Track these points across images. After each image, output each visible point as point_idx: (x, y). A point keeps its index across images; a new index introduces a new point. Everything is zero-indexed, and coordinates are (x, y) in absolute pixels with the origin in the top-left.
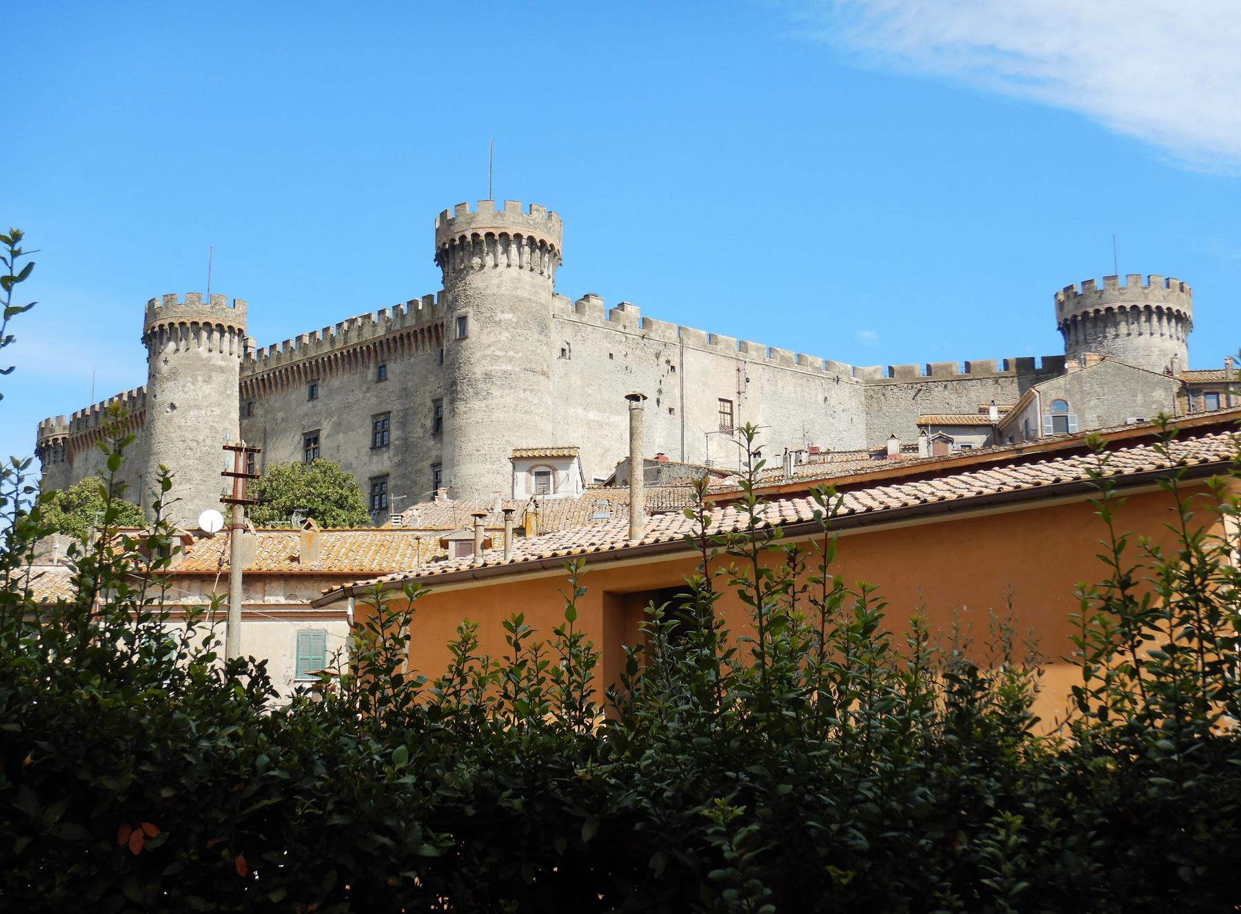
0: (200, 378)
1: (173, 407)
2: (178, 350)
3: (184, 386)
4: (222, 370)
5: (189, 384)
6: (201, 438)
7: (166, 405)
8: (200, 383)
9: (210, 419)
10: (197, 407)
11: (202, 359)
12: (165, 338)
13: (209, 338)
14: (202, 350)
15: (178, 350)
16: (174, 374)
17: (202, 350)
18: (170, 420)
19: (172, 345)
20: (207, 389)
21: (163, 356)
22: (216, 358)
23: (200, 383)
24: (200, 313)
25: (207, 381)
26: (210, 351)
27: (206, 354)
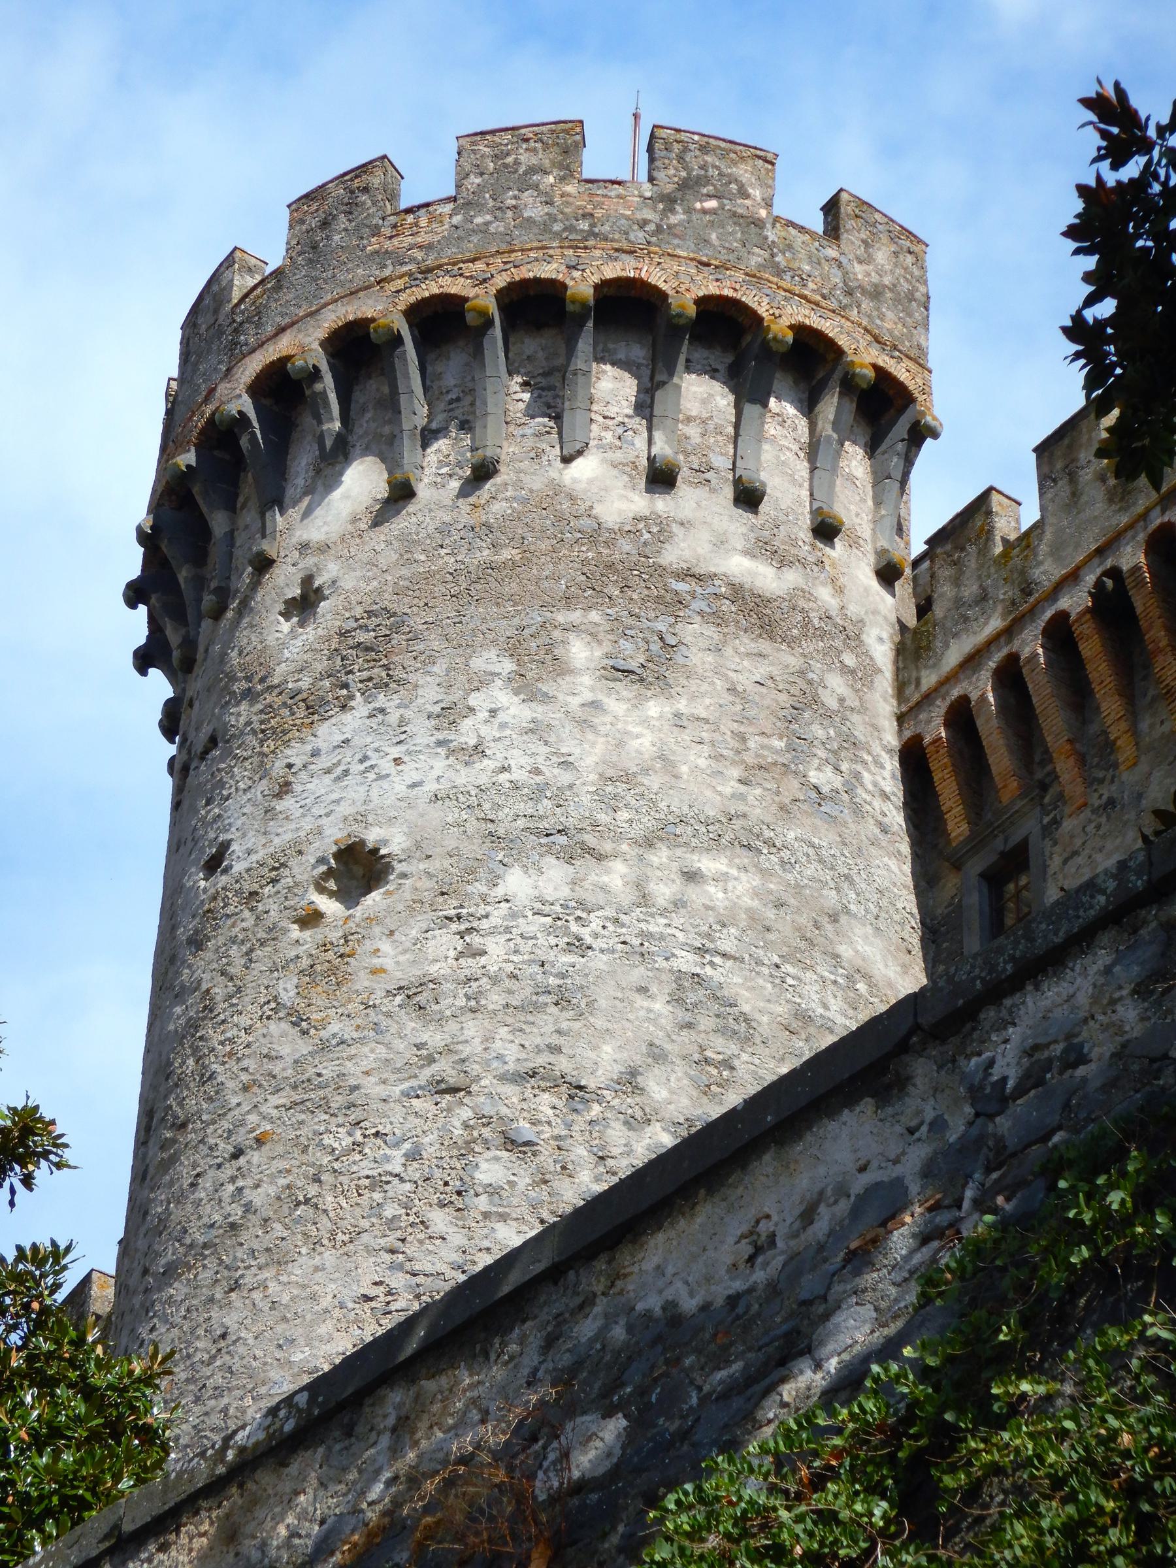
0: (579, 652)
1: (359, 868)
2: (401, 493)
3: (449, 714)
4: (756, 614)
5: (502, 696)
6: (602, 1062)
7: (303, 869)
8: (585, 686)
9: (679, 931)
10: (577, 847)
11: (596, 534)
12: (302, 461)
13: (645, 407)
14: (601, 480)
15: (401, 493)
16: (372, 656)
17: (601, 480)
18: (331, 968)
19: (362, 481)
20: (640, 724)
21: (284, 581)
22: (705, 532)
23: (585, 686)
24: (581, 236)
25: (646, 670)
26: (661, 478)
27: (623, 502)
